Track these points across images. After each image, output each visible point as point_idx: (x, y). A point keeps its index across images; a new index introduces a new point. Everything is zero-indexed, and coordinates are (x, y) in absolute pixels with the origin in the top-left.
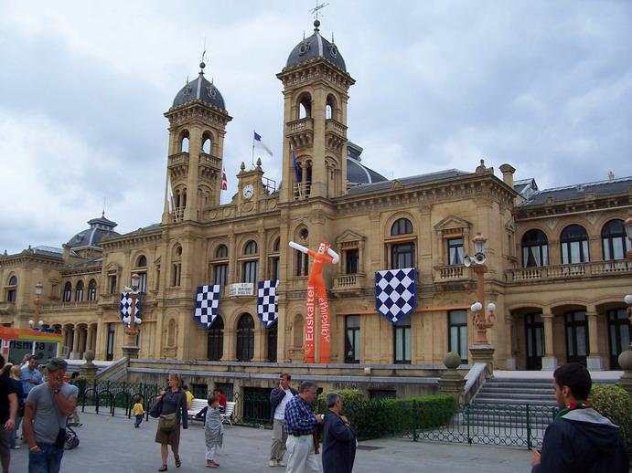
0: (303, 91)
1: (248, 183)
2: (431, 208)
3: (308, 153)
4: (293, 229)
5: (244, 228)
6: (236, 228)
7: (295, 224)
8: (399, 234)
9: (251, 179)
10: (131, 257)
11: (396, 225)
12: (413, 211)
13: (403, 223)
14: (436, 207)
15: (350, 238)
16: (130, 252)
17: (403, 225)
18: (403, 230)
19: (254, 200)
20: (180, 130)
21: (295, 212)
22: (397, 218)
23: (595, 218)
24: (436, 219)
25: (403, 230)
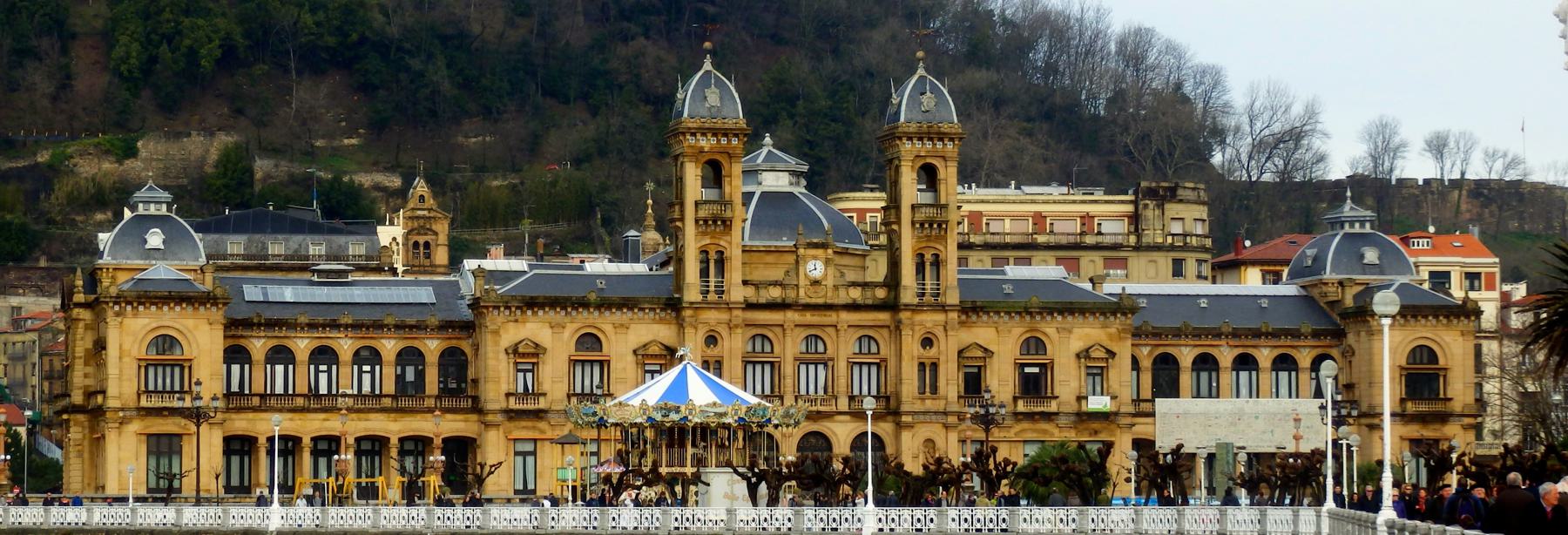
1: (815, 258)
2: (1070, 332)
3: (938, 246)
5: (809, 317)
8: (1028, 354)
9: (820, 252)
11: (1025, 346)
12: (1050, 329)
13: (1032, 343)
14: (1075, 330)
17: (1034, 345)
18: (1033, 351)
19: (830, 282)
21: (919, 317)
22: (1028, 335)
23: (1188, 349)
24: (1077, 345)
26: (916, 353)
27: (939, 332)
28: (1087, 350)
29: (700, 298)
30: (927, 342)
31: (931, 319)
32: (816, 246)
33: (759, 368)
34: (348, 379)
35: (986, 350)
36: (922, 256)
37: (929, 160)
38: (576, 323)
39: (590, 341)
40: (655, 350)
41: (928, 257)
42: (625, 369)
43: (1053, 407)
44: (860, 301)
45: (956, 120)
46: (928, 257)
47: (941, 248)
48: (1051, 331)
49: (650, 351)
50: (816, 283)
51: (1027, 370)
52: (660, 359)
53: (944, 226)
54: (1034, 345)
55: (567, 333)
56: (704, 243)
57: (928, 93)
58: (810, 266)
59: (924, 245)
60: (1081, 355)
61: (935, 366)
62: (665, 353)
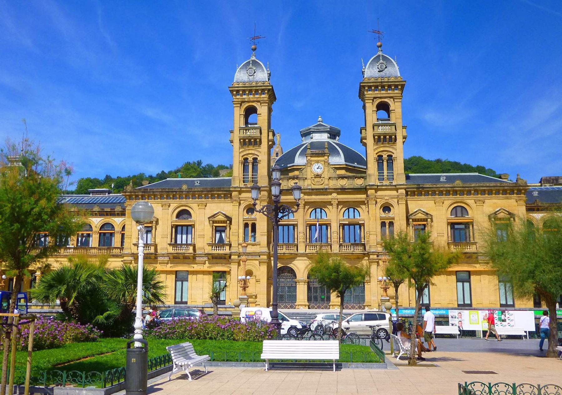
0: (383, 100)
1: (318, 162)
4: (379, 205)
6: (306, 197)
7: (380, 202)
10: (171, 209)
13: (459, 210)
15: (420, 216)
16: (169, 206)
17: (460, 210)
19: (326, 175)
20: (246, 105)
21: (379, 193)
25: (459, 214)
26: (378, 216)
27: (394, 202)
28: (495, 213)
29: (242, 185)
30: (386, 208)
31: (386, 195)
32: (318, 155)
33: (286, 228)
34: (186, 249)
35: (427, 214)
36: (380, 157)
37: (386, 100)
38: (175, 205)
39: (183, 213)
40: (221, 218)
41: (385, 156)
42: (203, 230)
43: (472, 249)
44: (347, 186)
45: (399, 75)
46: (385, 156)
47: (393, 151)
48: (471, 202)
49: (216, 219)
50: (318, 176)
51: (456, 226)
52: (224, 223)
53: (393, 137)
54: (460, 210)
55: (171, 209)
56: (245, 153)
57: (381, 61)
58: (315, 166)
59: (382, 149)
60: (492, 216)
61: (391, 224)
62: (225, 219)
